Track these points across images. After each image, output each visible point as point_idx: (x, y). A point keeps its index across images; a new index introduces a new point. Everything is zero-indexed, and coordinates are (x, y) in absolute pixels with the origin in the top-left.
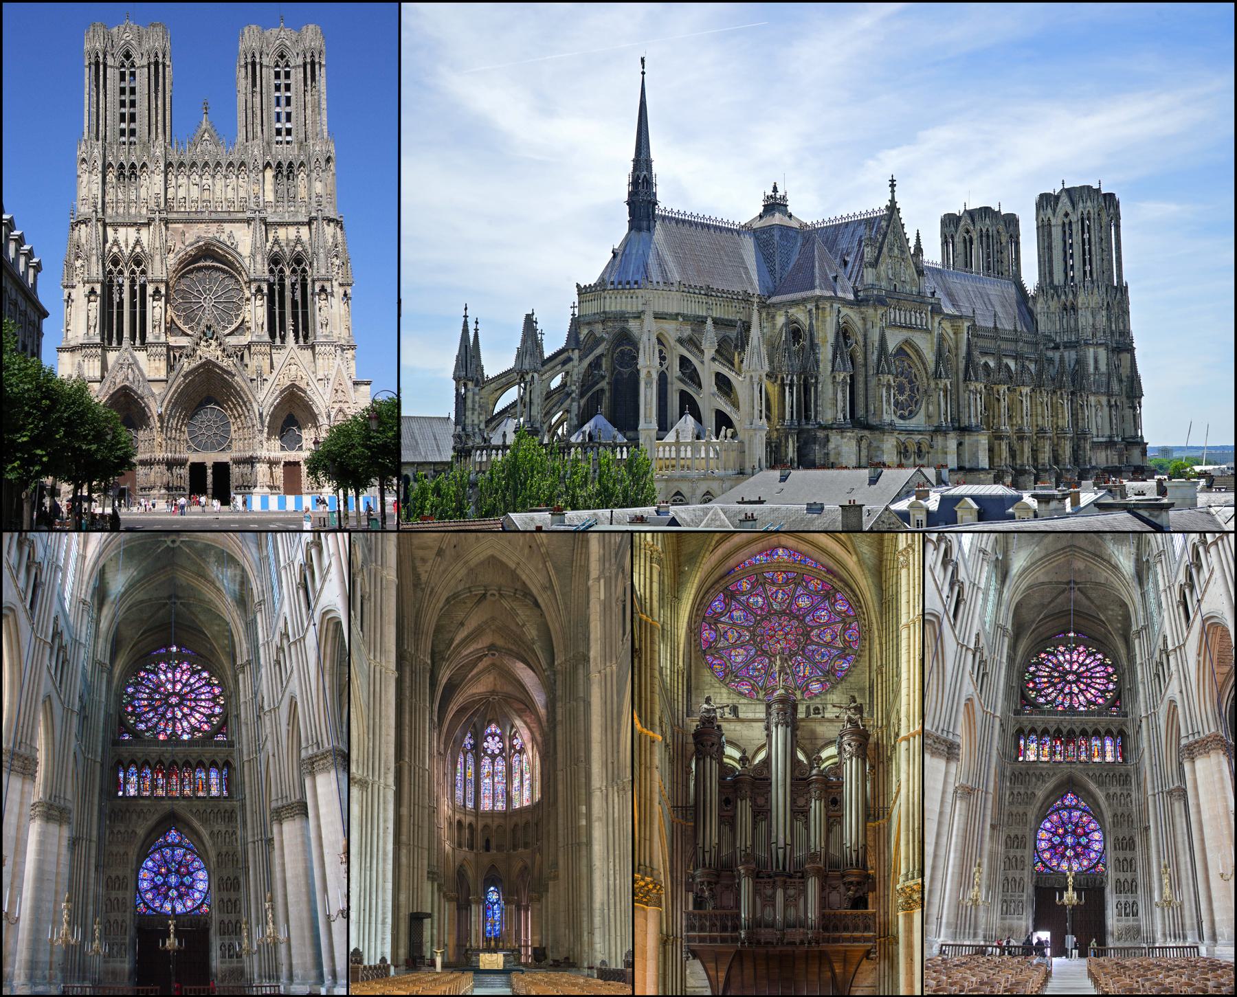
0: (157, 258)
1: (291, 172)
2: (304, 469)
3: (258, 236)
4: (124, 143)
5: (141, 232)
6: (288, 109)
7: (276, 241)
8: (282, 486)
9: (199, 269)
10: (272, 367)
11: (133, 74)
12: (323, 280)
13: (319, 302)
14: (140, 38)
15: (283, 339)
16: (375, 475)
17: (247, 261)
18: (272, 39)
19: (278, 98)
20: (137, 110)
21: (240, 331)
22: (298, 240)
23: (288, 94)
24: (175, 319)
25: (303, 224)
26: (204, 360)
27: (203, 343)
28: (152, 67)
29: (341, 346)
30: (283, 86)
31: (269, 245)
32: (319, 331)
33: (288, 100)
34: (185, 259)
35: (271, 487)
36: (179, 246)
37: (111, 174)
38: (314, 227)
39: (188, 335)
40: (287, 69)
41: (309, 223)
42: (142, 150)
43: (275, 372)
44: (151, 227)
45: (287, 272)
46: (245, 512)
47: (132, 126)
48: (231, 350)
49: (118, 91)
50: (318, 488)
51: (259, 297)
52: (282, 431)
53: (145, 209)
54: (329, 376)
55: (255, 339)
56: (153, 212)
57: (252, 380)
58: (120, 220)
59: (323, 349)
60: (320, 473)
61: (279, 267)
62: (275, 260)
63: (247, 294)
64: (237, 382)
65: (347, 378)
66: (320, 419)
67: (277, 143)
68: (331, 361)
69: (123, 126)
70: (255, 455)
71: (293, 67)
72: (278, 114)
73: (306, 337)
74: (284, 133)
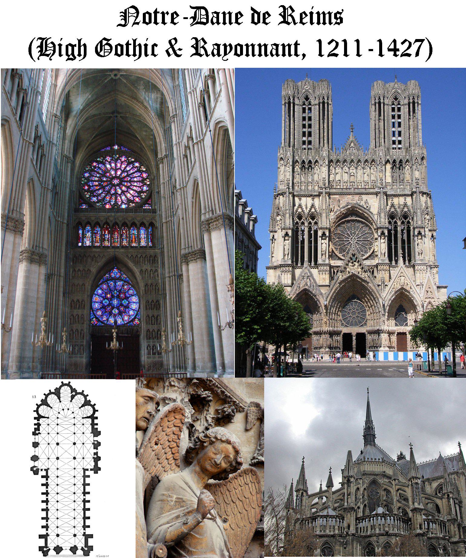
0: (324, 215)
1: (401, 165)
2: (409, 337)
3: (382, 202)
4: (305, 149)
5: (315, 200)
6: (399, 129)
7: (393, 205)
8: (396, 346)
9: (348, 221)
10: (390, 278)
11: (310, 109)
12: (420, 228)
13: (417, 241)
14: (314, 88)
15: (396, 261)
16: (449, 340)
17: (376, 217)
18: (390, 89)
19: (394, 123)
20: (312, 130)
21: (372, 257)
22: (405, 205)
23: (400, 121)
24: (334, 250)
25: (408, 195)
26: (351, 274)
27: (350, 264)
28: (321, 105)
29: (430, 266)
30: (396, 116)
31: (388, 207)
32: (417, 257)
33: (399, 124)
34: (340, 216)
35: (389, 347)
36: (337, 208)
37: (297, 167)
38: (414, 197)
39: (341, 259)
40: (399, 106)
41: (412, 195)
42: (315, 153)
43: (392, 281)
44: (321, 197)
45: (399, 223)
46: (374, 362)
47: (310, 139)
48: (366, 268)
49: (301, 118)
50: (416, 348)
51: (383, 237)
52: (396, 315)
53: (317, 187)
54: (423, 283)
55: (380, 262)
56: (321, 188)
57: (378, 285)
58: (302, 193)
59: (419, 267)
60: (418, 339)
61: (394, 220)
62: (392, 216)
63: (376, 236)
64: (370, 287)
65: (433, 284)
66: (418, 308)
67: (393, 148)
68: (424, 274)
69: (304, 139)
70: (380, 329)
71: (403, 105)
72: (394, 132)
73: (410, 261)
74: (397, 143)
